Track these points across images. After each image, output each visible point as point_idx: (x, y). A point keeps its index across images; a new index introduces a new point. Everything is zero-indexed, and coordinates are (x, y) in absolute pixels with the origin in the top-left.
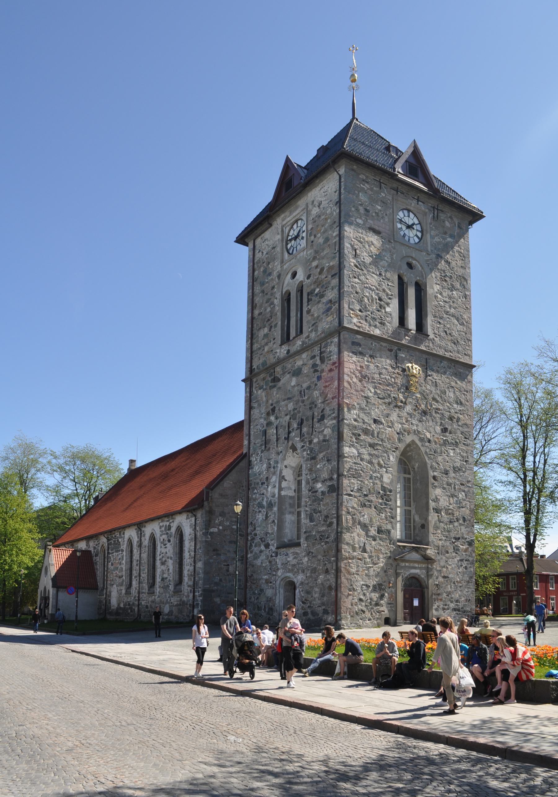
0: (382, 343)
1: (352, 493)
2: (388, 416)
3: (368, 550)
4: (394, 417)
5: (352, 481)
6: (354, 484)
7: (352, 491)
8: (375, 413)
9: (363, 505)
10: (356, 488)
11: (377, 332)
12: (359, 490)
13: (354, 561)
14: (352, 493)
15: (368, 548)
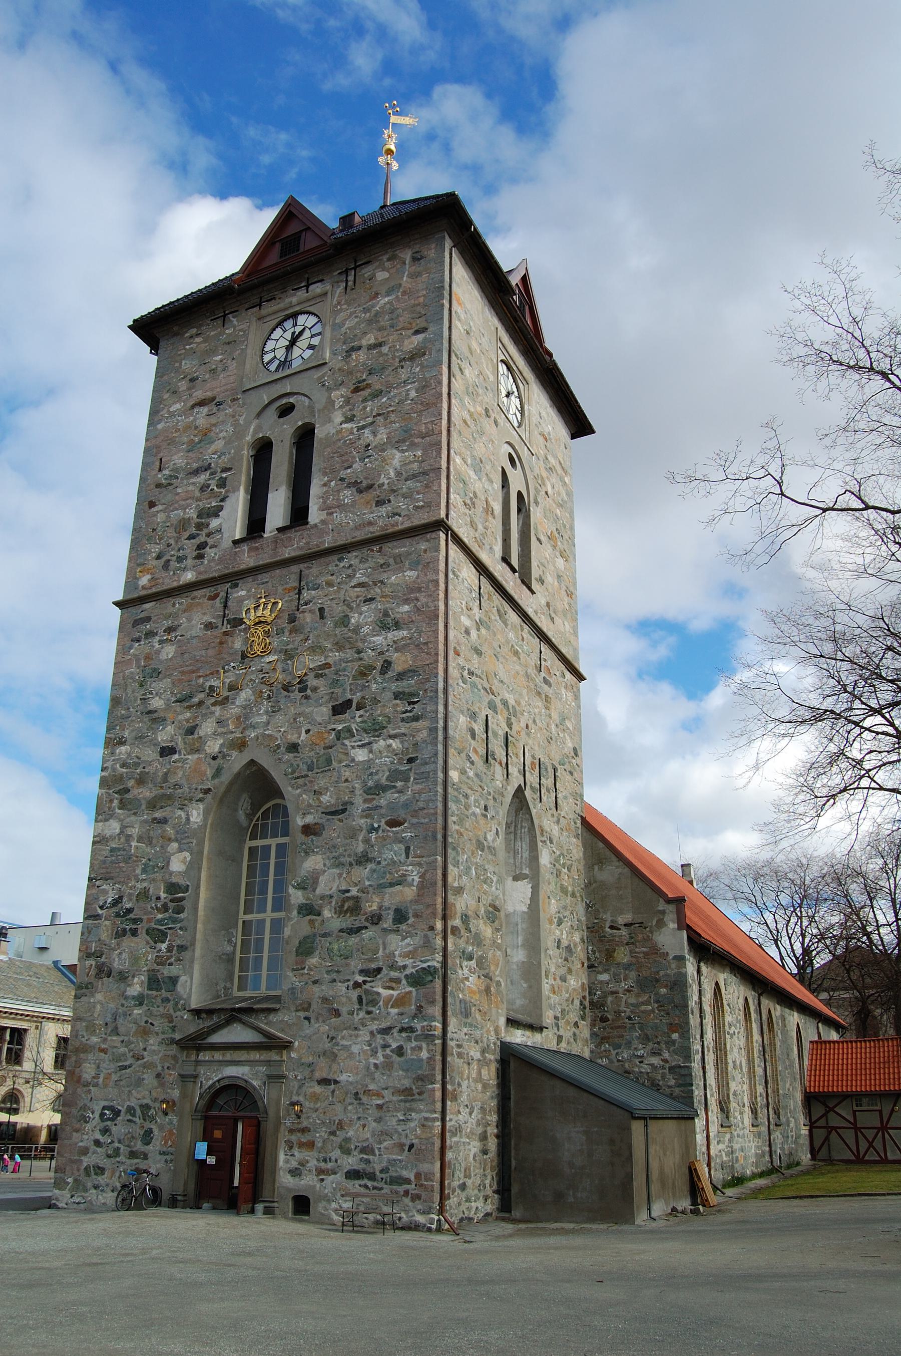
0: (195, 593)
1: (100, 912)
2: (191, 731)
3: (122, 1030)
4: (207, 728)
5: (104, 887)
6: (105, 892)
7: (101, 908)
8: (165, 735)
9: (120, 934)
10: (110, 900)
11: (189, 576)
12: (117, 902)
13: (90, 1056)
14: (100, 912)
15: (124, 1025)
